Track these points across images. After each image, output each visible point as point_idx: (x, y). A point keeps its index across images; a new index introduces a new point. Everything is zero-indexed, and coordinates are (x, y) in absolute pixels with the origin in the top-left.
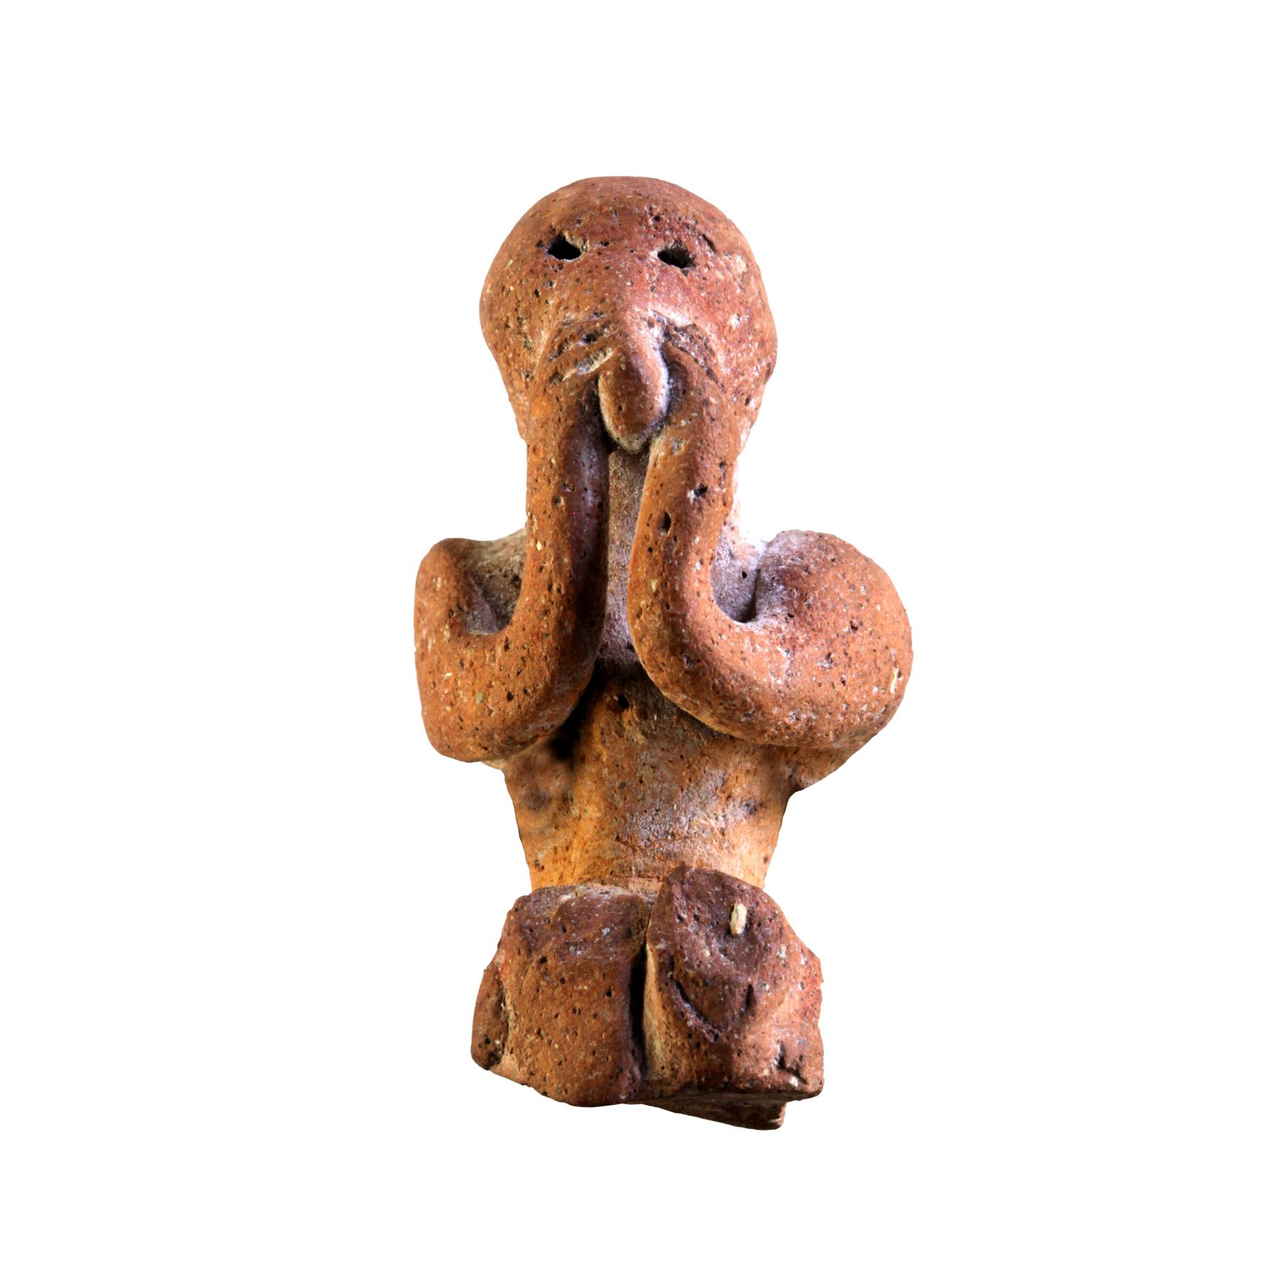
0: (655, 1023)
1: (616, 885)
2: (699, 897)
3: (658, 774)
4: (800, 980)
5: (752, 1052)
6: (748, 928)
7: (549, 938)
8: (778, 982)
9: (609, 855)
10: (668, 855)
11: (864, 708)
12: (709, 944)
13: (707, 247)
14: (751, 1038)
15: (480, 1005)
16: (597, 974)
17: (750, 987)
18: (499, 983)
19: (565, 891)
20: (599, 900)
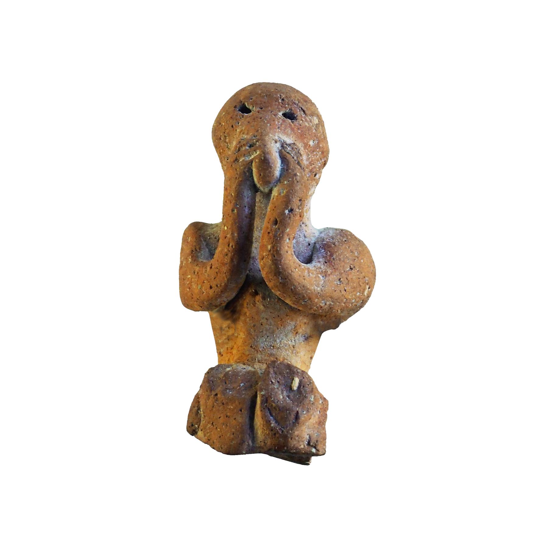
0: (259, 424)
1: (249, 365)
2: (280, 374)
3: (269, 322)
4: (319, 410)
5: (297, 438)
6: (299, 387)
7: (219, 386)
8: (309, 410)
9: (247, 353)
10: (271, 355)
11: (353, 301)
12: (282, 393)
13: (302, 113)
14: (296, 433)
15: (191, 410)
16: (237, 402)
17: (298, 412)
18: (199, 402)
19: (228, 367)
20: (241, 372)
